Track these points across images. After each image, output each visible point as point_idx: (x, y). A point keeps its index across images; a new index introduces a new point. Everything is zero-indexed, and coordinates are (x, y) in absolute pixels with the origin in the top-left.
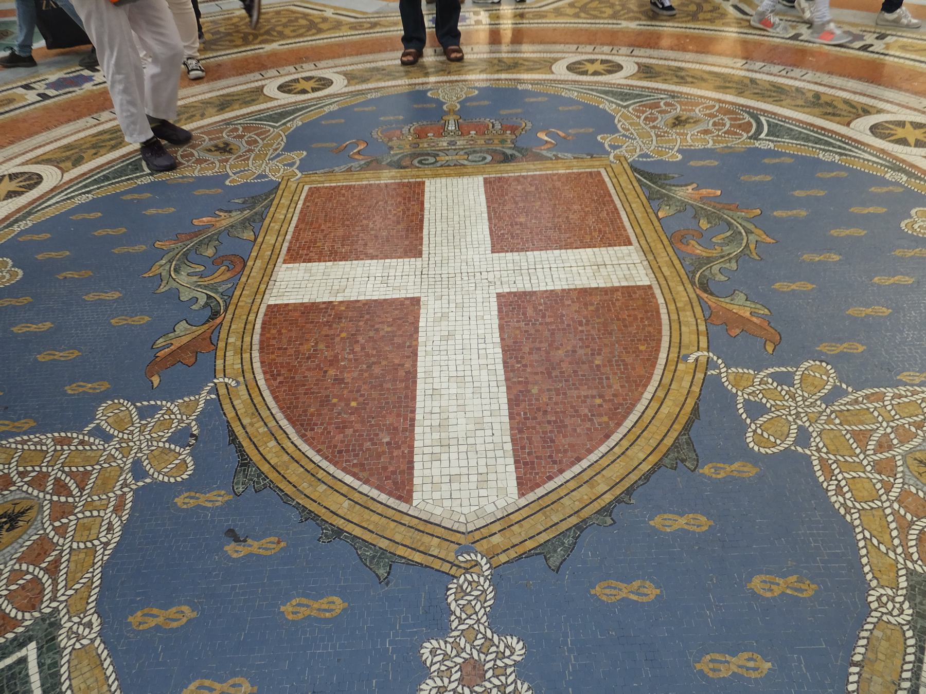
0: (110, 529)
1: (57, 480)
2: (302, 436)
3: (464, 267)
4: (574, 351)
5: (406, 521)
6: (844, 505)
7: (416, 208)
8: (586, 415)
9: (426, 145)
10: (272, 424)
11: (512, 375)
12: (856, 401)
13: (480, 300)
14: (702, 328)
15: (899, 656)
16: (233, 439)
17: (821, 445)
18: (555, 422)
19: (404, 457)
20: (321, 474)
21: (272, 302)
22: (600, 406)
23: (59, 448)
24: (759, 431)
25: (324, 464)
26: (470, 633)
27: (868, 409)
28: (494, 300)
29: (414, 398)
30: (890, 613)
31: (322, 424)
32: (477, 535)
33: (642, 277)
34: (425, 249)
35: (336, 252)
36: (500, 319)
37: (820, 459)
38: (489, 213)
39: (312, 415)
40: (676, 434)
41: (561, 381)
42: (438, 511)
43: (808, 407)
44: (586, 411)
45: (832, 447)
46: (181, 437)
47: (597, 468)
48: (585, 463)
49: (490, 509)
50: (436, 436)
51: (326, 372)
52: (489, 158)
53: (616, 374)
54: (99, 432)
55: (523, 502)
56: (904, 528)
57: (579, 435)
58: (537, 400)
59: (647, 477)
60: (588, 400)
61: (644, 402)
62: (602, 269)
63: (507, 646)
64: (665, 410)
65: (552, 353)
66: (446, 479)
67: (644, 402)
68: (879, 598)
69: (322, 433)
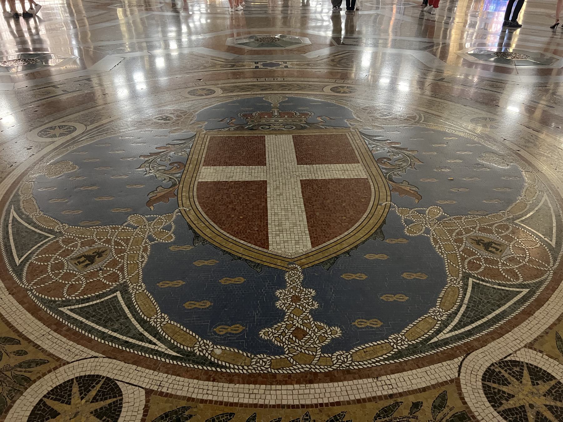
0: (143, 257)
1: (115, 242)
2: (221, 228)
3: (285, 170)
4: (334, 201)
5: (267, 254)
6: (441, 252)
7: (262, 147)
8: (339, 222)
9: (264, 121)
10: (207, 223)
11: (308, 208)
12: (450, 220)
13: (293, 182)
14: (389, 194)
15: (456, 296)
16: (191, 228)
17: (434, 233)
18: (326, 224)
19: (264, 234)
20: (230, 240)
21: (200, 180)
22: (345, 219)
23: (113, 230)
24: (410, 229)
25: (231, 237)
26: (295, 288)
27: (455, 222)
28: (299, 182)
29: (267, 216)
30: (455, 284)
31: (228, 224)
32: (296, 259)
33: (364, 175)
34: (267, 162)
35: (227, 163)
36: (302, 189)
37: (434, 238)
38: (295, 149)
39: (224, 221)
40: (376, 229)
41: (328, 211)
42: (280, 252)
43: (430, 221)
44: (339, 221)
45: (438, 234)
46: (168, 228)
47: (343, 239)
48: (338, 238)
49: (301, 251)
50: (277, 228)
51: (228, 206)
52: (295, 128)
53: (352, 209)
54: (129, 225)
55: (314, 249)
56: (463, 259)
57: (336, 229)
58: (319, 217)
59: (363, 242)
60: (340, 218)
61: (363, 218)
62: (347, 172)
63: (309, 292)
64: (371, 221)
65: (324, 201)
66: (283, 242)
67: (363, 218)
68: (451, 280)
69: (229, 227)
